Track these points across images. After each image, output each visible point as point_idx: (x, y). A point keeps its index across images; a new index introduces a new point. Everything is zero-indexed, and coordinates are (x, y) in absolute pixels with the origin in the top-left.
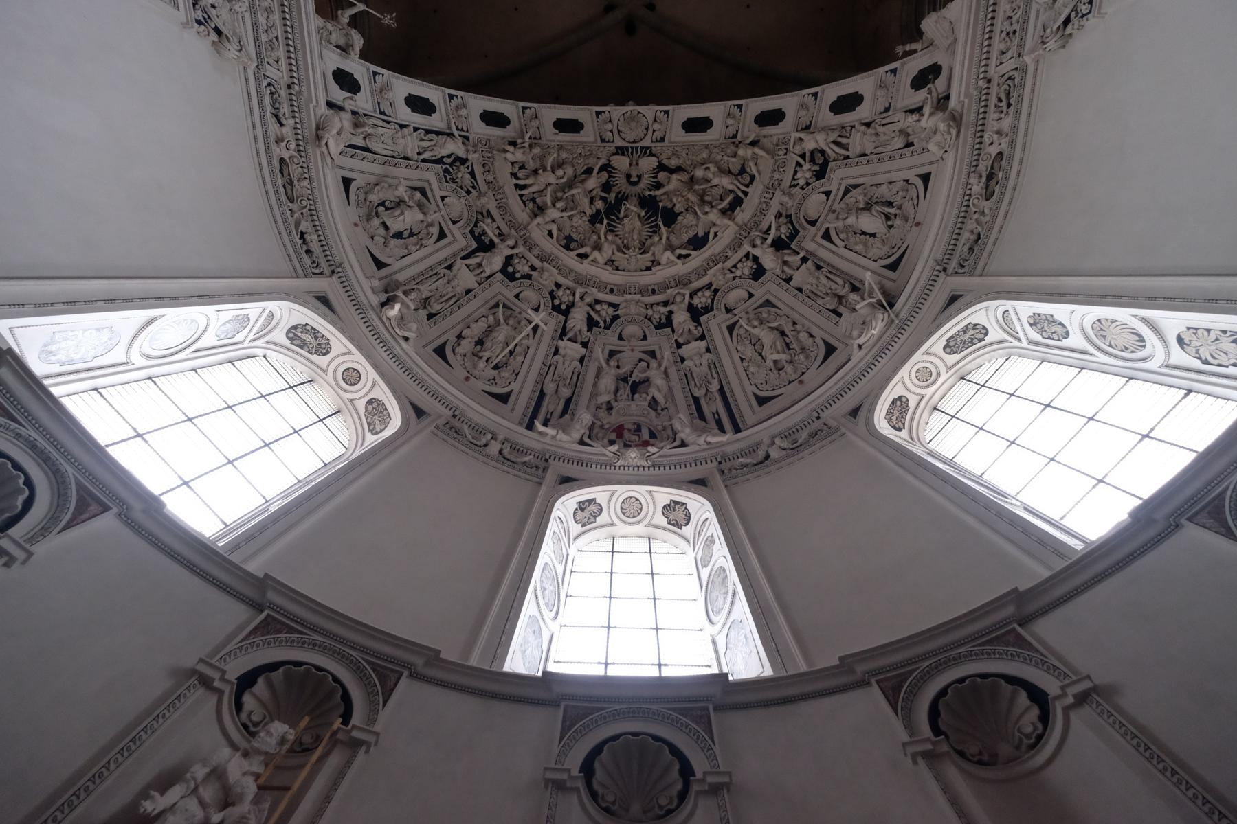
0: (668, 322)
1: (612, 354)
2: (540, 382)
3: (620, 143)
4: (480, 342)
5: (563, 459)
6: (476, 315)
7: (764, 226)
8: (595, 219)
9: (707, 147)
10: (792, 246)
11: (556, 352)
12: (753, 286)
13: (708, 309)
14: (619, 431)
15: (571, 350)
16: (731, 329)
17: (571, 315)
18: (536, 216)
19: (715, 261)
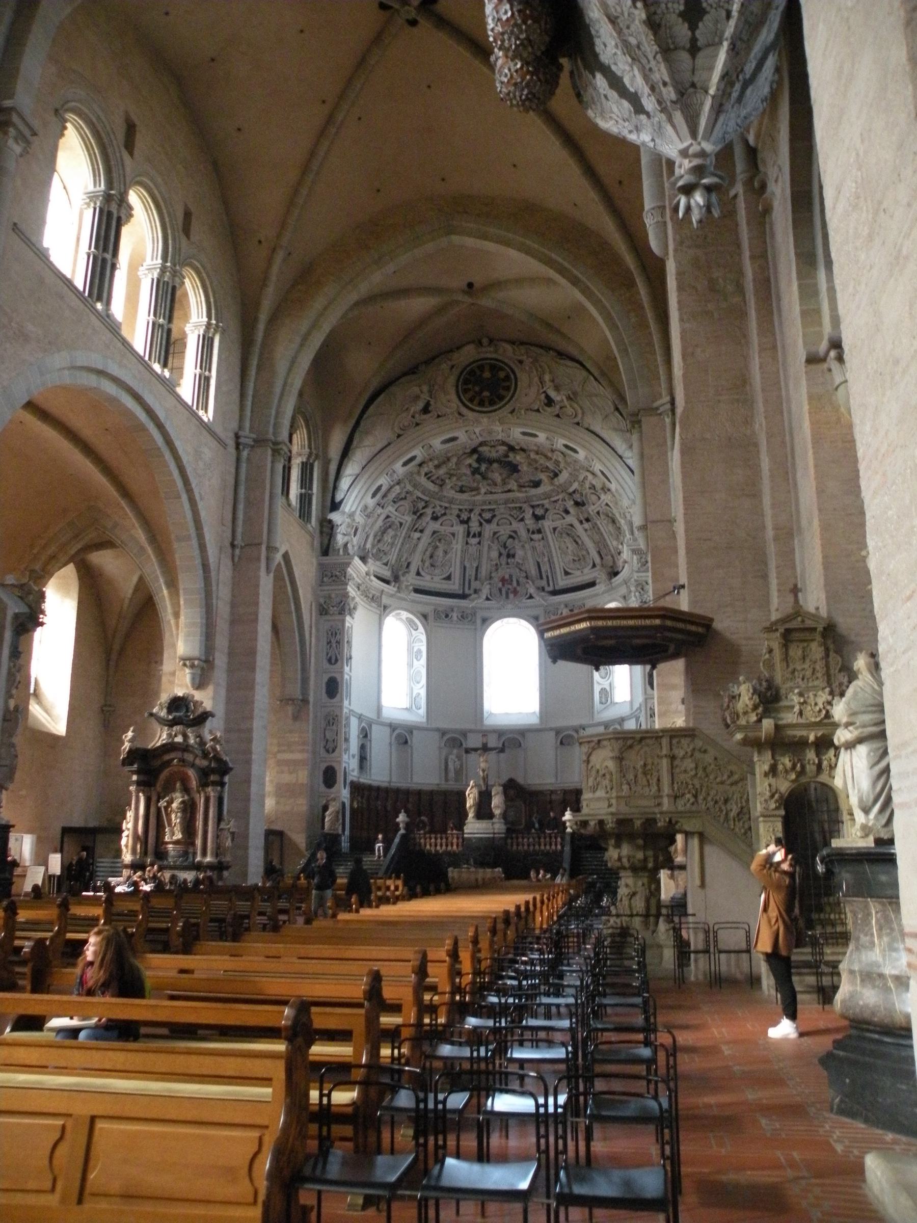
0: (522, 520)
1: (495, 533)
2: (462, 562)
3: (481, 439)
4: (431, 557)
5: (481, 609)
6: (426, 545)
7: (571, 490)
8: (473, 473)
9: (535, 445)
10: (583, 508)
11: (467, 543)
12: (564, 515)
13: (542, 517)
14: (503, 580)
15: (474, 541)
16: (555, 529)
17: (471, 524)
18: (441, 486)
19: (547, 496)
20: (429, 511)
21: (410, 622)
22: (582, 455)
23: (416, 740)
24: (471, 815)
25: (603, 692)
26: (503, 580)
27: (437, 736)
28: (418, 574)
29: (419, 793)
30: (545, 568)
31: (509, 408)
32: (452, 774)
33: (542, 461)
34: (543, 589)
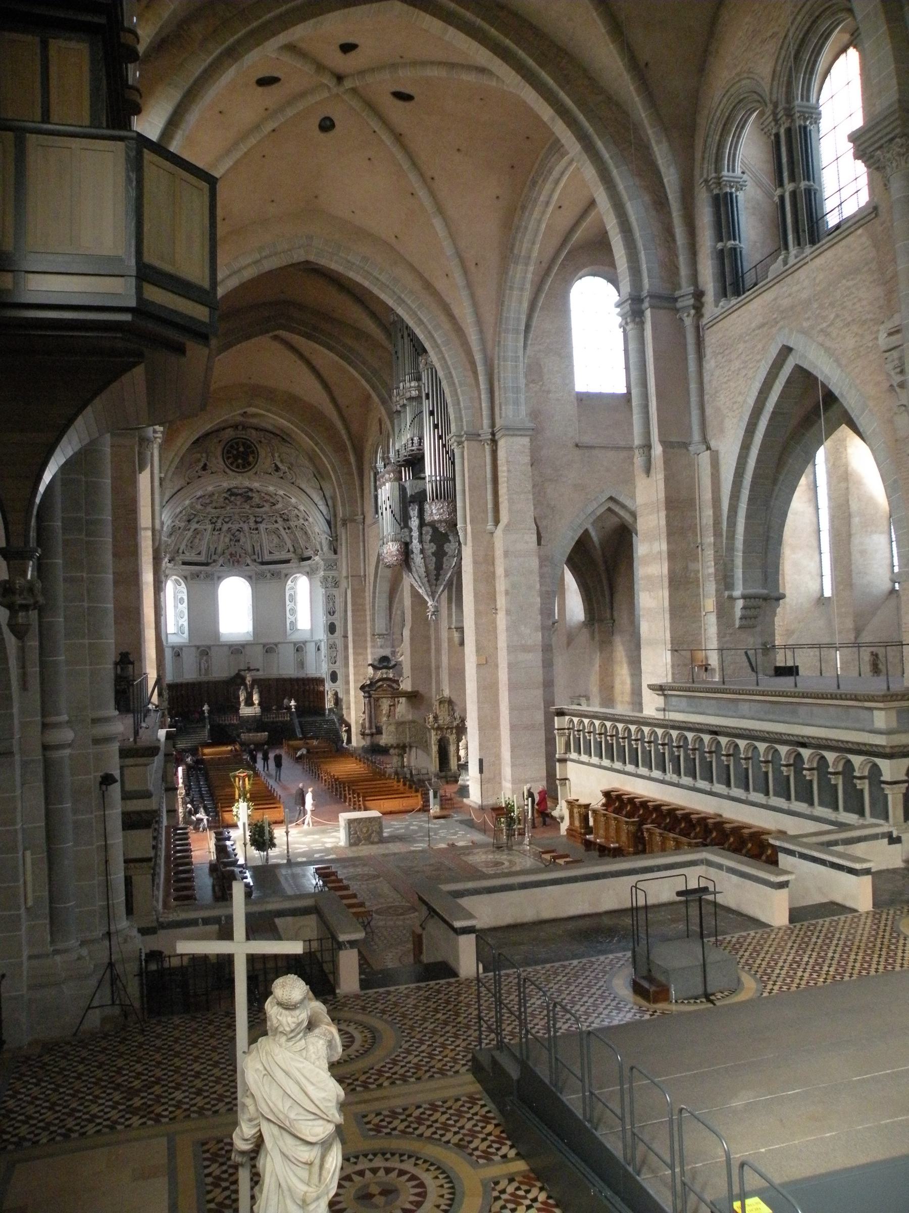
2: (208, 544)
13: (261, 522)
14: (231, 554)
15: (217, 533)
19: (266, 513)
20: (196, 520)
21: (176, 581)
22: (293, 500)
23: (184, 655)
24: (242, 704)
25: (291, 623)
26: (231, 554)
27: (194, 649)
28: (183, 553)
29: (187, 684)
30: (257, 548)
31: (254, 470)
32: (203, 671)
33: (267, 497)
34: (255, 561)
